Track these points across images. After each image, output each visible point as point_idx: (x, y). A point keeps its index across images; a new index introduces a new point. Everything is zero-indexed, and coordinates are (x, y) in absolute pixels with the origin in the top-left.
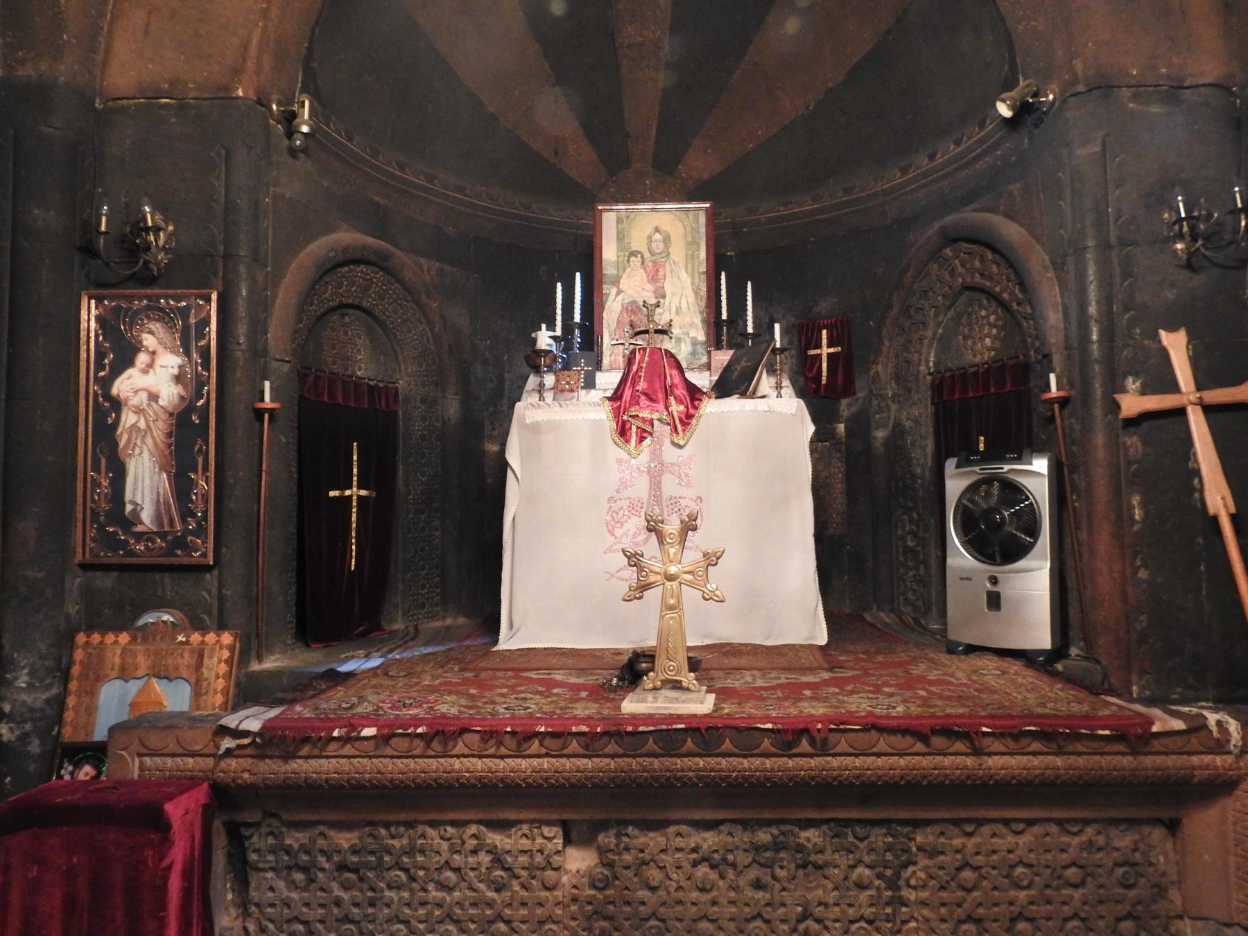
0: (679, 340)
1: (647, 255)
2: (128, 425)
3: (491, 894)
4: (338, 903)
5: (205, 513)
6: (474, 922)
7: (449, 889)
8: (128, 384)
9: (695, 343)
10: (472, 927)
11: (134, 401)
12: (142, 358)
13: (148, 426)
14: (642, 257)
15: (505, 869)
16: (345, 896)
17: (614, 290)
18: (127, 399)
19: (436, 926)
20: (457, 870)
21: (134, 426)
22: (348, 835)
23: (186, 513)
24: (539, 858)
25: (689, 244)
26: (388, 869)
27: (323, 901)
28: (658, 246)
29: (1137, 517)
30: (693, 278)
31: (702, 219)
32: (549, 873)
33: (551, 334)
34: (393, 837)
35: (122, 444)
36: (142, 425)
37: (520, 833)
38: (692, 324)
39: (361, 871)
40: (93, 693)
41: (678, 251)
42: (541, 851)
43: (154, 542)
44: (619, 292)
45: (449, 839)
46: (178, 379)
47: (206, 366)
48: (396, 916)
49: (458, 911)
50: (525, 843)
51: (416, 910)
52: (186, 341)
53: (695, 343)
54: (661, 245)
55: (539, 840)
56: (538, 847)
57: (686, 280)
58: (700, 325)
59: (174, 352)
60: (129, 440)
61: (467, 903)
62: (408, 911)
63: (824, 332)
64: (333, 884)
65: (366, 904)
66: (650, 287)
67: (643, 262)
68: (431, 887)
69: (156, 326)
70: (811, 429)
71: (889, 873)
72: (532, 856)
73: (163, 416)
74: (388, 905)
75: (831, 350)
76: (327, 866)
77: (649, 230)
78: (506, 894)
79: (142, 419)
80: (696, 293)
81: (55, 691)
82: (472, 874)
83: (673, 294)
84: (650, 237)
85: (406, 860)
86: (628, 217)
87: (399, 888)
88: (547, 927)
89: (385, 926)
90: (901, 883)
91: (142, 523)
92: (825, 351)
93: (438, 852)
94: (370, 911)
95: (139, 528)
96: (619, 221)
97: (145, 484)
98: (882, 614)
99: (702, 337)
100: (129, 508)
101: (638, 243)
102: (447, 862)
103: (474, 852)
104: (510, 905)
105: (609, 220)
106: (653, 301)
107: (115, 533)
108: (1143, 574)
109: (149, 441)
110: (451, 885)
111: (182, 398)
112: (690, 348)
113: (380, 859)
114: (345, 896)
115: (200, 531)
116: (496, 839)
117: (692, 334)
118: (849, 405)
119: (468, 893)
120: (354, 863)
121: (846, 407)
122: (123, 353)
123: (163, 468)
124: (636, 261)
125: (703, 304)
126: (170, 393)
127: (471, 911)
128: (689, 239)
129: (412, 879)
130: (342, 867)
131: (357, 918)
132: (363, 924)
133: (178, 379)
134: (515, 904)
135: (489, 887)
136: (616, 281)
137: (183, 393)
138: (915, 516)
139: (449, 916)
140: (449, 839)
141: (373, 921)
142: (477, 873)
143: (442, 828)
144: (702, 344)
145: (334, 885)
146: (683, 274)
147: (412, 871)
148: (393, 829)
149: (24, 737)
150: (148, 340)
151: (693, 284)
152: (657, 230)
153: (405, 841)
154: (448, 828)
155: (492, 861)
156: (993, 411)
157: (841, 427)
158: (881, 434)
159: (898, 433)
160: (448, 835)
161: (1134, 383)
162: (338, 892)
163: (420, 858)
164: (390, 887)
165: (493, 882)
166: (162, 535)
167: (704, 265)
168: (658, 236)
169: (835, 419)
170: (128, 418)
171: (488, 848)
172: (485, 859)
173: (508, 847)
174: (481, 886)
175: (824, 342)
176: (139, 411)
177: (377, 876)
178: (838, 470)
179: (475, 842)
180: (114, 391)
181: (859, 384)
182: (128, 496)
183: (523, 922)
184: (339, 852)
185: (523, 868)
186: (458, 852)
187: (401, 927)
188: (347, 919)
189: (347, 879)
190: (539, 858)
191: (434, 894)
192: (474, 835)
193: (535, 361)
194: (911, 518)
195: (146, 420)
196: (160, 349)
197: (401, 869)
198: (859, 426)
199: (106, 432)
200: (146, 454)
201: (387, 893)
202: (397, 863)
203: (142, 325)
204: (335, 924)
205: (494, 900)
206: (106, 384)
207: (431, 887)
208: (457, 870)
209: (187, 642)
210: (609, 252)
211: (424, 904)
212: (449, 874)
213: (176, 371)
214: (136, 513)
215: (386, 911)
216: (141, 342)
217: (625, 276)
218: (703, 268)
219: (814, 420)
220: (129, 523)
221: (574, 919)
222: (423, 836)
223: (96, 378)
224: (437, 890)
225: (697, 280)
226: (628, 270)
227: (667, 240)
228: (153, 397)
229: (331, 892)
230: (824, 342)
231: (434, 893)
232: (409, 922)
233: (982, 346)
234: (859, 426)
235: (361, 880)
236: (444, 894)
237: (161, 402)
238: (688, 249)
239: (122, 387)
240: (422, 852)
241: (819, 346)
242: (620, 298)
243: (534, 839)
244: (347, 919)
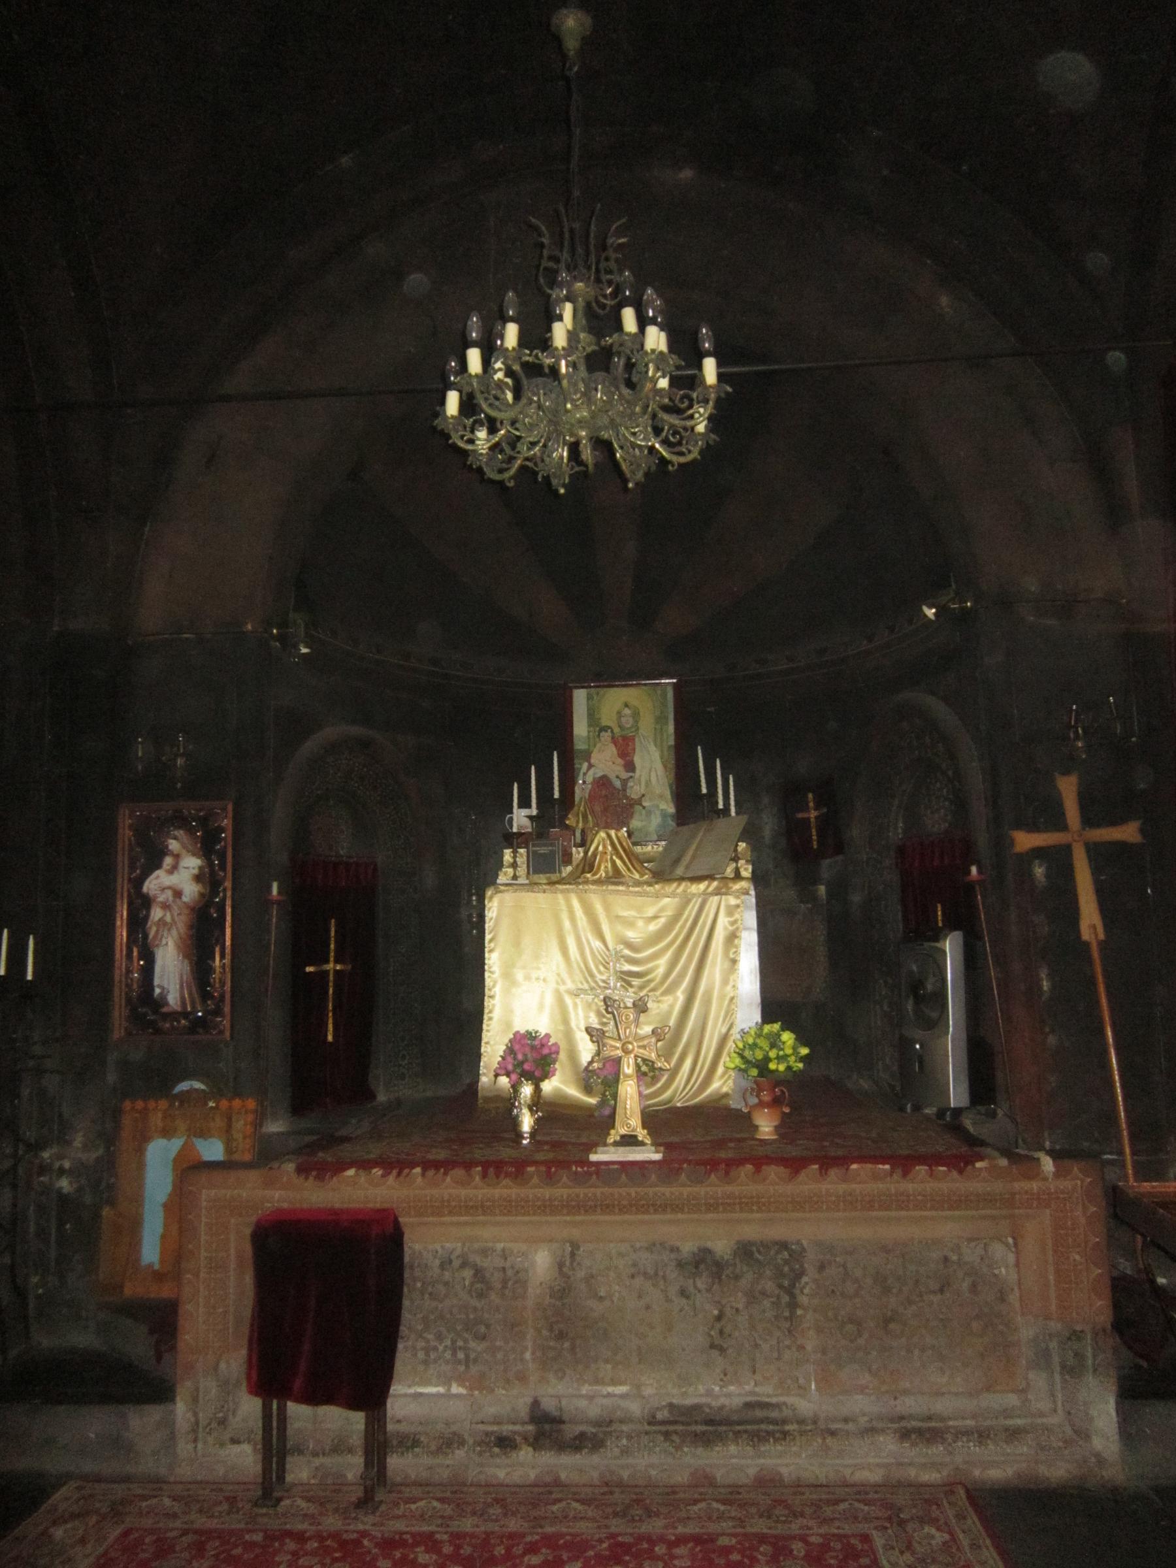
0: (649, 813)
1: (617, 730)
2: (157, 919)
5: (222, 997)
8: (157, 883)
9: (664, 815)
11: (161, 899)
12: (168, 861)
13: (173, 920)
17: (585, 765)
18: (155, 897)
21: (162, 922)
23: (205, 996)
28: (628, 722)
29: (1045, 988)
30: (662, 751)
31: (670, 694)
33: (525, 812)
35: (151, 937)
36: (168, 919)
38: (661, 796)
40: (140, 1151)
41: (647, 724)
43: (179, 1022)
44: (590, 766)
46: (198, 878)
47: (223, 867)
52: (207, 847)
53: (664, 815)
54: (631, 720)
57: (656, 755)
59: (194, 855)
60: (157, 931)
66: (620, 761)
69: (180, 833)
71: (786, 1283)
73: (186, 911)
77: (618, 705)
79: (168, 914)
80: (665, 767)
81: (101, 1152)
84: (619, 713)
86: (598, 694)
90: (797, 1291)
91: (167, 1004)
95: (165, 1010)
96: (589, 698)
97: (170, 970)
98: (861, 1081)
99: (671, 809)
100: (157, 991)
101: (607, 717)
105: (580, 697)
106: (624, 775)
107: (145, 1015)
108: (1052, 1040)
109: (174, 932)
111: (202, 895)
115: (218, 1012)
117: (663, 806)
121: (828, 867)
122: (154, 858)
123: (185, 956)
124: (606, 735)
125: (672, 775)
126: (191, 890)
133: (198, 878)
136: (587, 755)
137: (203, 891)
138: (890, 981)
144: (672, 816)
146: (652, 748)
149: (80, 1190)
150: (173, 845)
152: (626, 705)
156: (937, 887)
157: (822, 889)
158: (856, 898)
166: (185, 1014)
168: (627, 711)
169: (816, 881)
170: (156, 913)
172: (468, 1273)
176: (165, 906)
180: (145, 889)
182: (156, 982)
193: (512, 840)
194: (886, 982)
195: (172, 916)
196: (184, 852)
199: (138, 923)
200: (171, 943)
203: (168, 832)
206: (138, 882)
208: (446, 1284)
209: (217, 1108)
210: (580, 728)
213: (196, 871)
214: (163, 997)
216: (167, 846)
217: (596, 750)
218: (672, 742)
220: (157, 1004)
223: (130, 880)
225: (666, 753)
226: (598, 745)
227: (636, 715)
228: (178, 894)
233: (936, 821)
234: (838, 890)
237: (185, 899)
239: (152, 886)
242: (591, 772)
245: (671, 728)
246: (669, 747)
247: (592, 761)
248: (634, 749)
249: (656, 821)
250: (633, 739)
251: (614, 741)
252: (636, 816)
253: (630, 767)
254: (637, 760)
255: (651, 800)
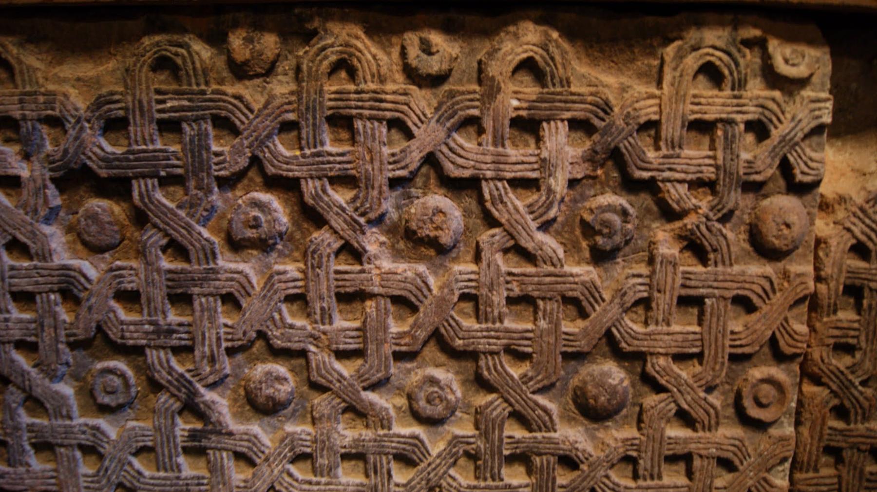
3: (582, 271)
4: (70, 290)
6: (520, 357)
7: (437, 249)
10: (516, 371)
15: (630, 185)
16: (91, 268)
19: (394, 369)
20: (464, 187)
22: (87, 69)
24: (749, 152)
26: (227, 183)
27: (25, 285)
32: (783, 204)
34: (240, 71)
37: (692, 62)
39: (137, 188)
42: (759, 129)
45: (435, 81)
48: (262, 335)
49: (469, 323)
50: (714, 103)
51: (326, 316)
55: (756, 89)
56: (752, 113)
61: (499, 298)
62: (300, 322)
64: (47, 229)
65: (159, 295)
68: (373, 242)
72: (729, 142)
74: (230, 300)
76: (24, 171)
78: (629, 274)
82: (518, 201)
85: (282, 148)
87: (264, 245)
88: (757, 373)
89: (227, 365)
93: (398, 125)
94: (173, 317)
102: (431, 160)
103: (528, 126)
104: (645, 303)
110: (446, 239)
113: (200, 145)
114: (91, 268)
116: (594, 78)
119: (503, 264)
120: (108, 161)
127: (508, 323)
129: (312, 216)
130: (74, 178)
131: (135, 339)
132: (152, 356)
134: (663, 302)
135: (572, 248)
139: (437, 337)
140: (435, 81)
141: (183, 351)
142: (533, 197)
143: (412, 39)
145: (56, 238)
147: (310, 188)
148: (236, 41)
153: (281, 87)
154: (436, 39)
155: (591, 158)
160: (434, 65)
162: (61, 250)
163: (331, 145)
164: (236, 245)
165: (588, 230)
171: (578, 112)
173: (648, 111)
174: (549, 242)
177: (191, 206)
179: (531, 90)
183: (680, 358)
184: (56, 122)
185: (696, 184)
186: (473, 124)
187: (280, 369)
188: (100, 341)
189: (93, 217)
190: (749, 152)
191: (386, 265)
192: (528, 66)
197: (275, 183)
201: (226, 262)
202: (255, 161)
204: (68, 355)
205: (592, 289)
207: (373, 242)
211: (351, 298)
212: (438, 199)
215: (225, 318)
221: (847, 349)
222: (345, 66)
224: (397, 255)
229: (45, 255)
231: (387, 264)
232: (303, 354)
235: (140, 218)
236: (422, 268)
240: (342, 122)
243: (740, 84)
244: (100, 341)
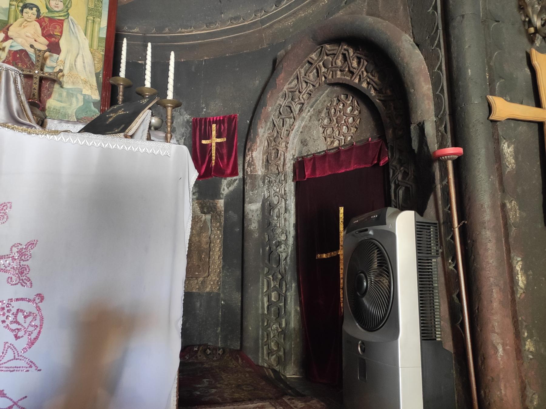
0: (70, 94)
1: (44, 11)
9: (87, 100)
14: (38, 11)
25: (90, 10)
29: (521, 284)
38: (86, 82)
53: (87, 100)
57: (85, 42)
58: (95, 83)
63: (214, 126)
66: (45, 41)
67: (38, 16)
70: (194, 175)
75: (219, 140)
83: (68, 52)
92: (215, 141)
99: (96, 96)
112: (81, 104)
117: (87, 91)
118: (229, 185)
121: (227, 186)
124: (31, 14)
128: (92, 6)
144: (95, 104)
151: (91, 46)
159: (268, 208)
161: (509, 147)
167: (105, 31)
175: (214, 133)
178: (216, 236)
181: (240, 168)
198: (239, 200)
219: (198, 167)
226: (20, 20)
230: (214, 133)
238: (89, 15)
241: (209, 137)
245: (104, 23)
246: (100, 39)
247: (10, 33)
248: (61, 32)
249: (76, 104)
250: (61, 23)
251: (39, 19)
252: (55, 95)
253: (54, 48)
254: (63, 43)
255: (73, 83)
